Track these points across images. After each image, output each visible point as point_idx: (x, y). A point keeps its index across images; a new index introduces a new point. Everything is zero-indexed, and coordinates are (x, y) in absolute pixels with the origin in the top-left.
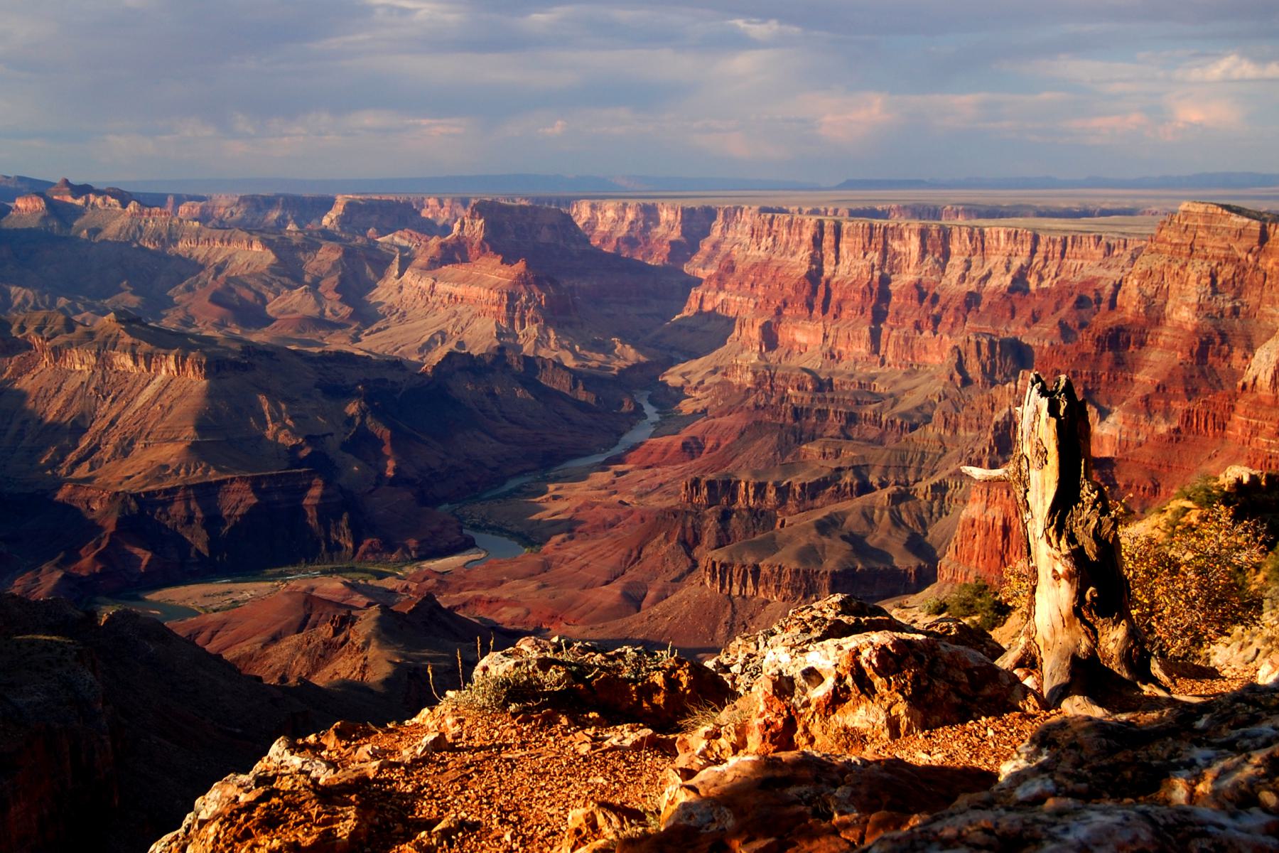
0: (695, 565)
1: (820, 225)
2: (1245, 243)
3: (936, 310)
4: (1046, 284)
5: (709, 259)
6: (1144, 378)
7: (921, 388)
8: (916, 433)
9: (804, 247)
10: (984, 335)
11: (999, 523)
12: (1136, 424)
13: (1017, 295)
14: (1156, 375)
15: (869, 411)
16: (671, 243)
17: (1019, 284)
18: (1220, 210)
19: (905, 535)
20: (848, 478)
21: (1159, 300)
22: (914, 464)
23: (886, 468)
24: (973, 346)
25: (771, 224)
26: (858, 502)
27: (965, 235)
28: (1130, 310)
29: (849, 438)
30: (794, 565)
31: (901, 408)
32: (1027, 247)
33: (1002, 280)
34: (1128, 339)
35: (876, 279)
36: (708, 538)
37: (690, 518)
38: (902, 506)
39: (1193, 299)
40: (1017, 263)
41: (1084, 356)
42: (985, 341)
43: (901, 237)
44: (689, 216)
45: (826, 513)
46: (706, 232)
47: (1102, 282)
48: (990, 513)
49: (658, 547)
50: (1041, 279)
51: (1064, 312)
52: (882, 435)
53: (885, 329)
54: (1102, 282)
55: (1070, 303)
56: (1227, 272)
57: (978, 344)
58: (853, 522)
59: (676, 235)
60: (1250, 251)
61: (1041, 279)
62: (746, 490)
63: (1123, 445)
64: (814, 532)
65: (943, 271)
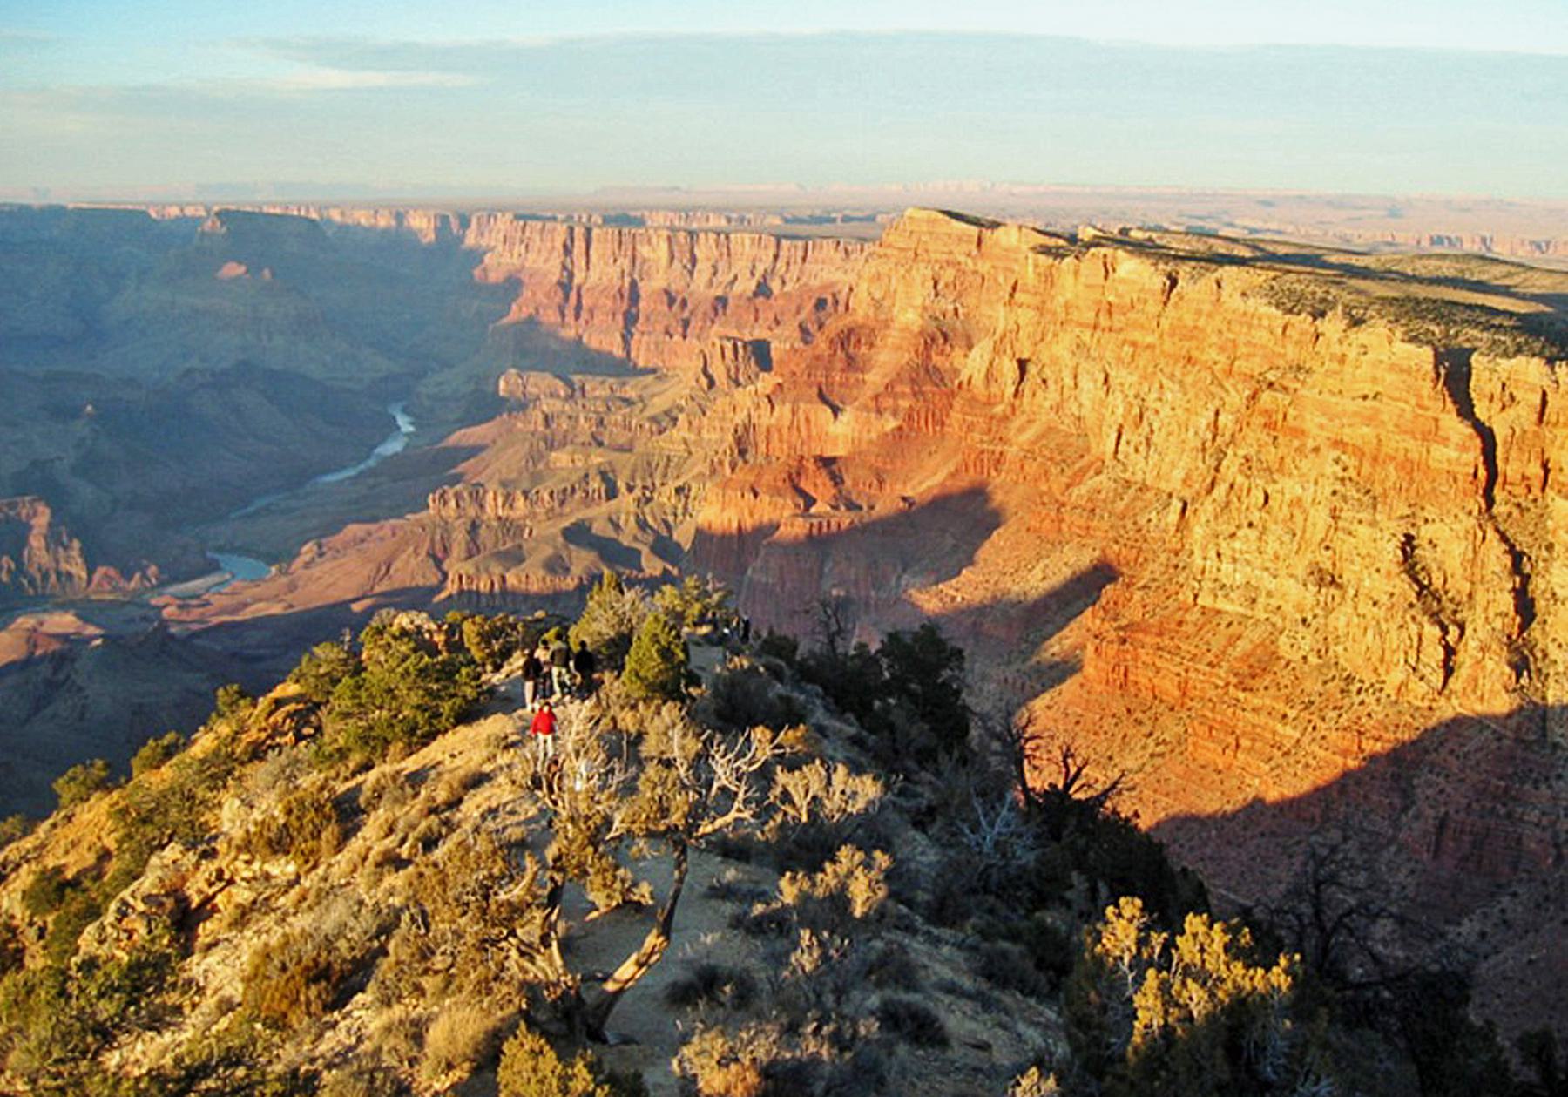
0: (445, 575)
2: (965, 247)
3: (686, 314)
6: (874, 379)
7: (668, 393)
9: (555, 254)
10: (728, 339)
12: (868, 422)
13: (761, 299)
14: (886, 375)
17: (763, 290)
18: (941, 216)
19: (651, 539)
20: (596, 484)
21: (886, 303)
22: (660, 469)
23: (634, 472)
25: (523, 231)
26: (605, 507)
27: (712, 242)
28: (861, 313)
29: (600, 444)
31: (649, 413)
33: (747, 285)
34: (859, 341)
35: (627, 285)
37: (438, 531)
38: (647, 509)
39: (918, 302)
41: (817, 358)
42: (729, 345)
45: (573, 520)
47: (839, 286)
49: (407, 562)
50: (784, 283)
51: (803, 316)
52: (631, 441)
53: (637, 336)
54: (839, 286)
55: (809, 306)
56: (948, 275)
58: (600, 528)
60: (969, 255)
62: (495, 499)
64: (560, 540)
65: (691, 273)
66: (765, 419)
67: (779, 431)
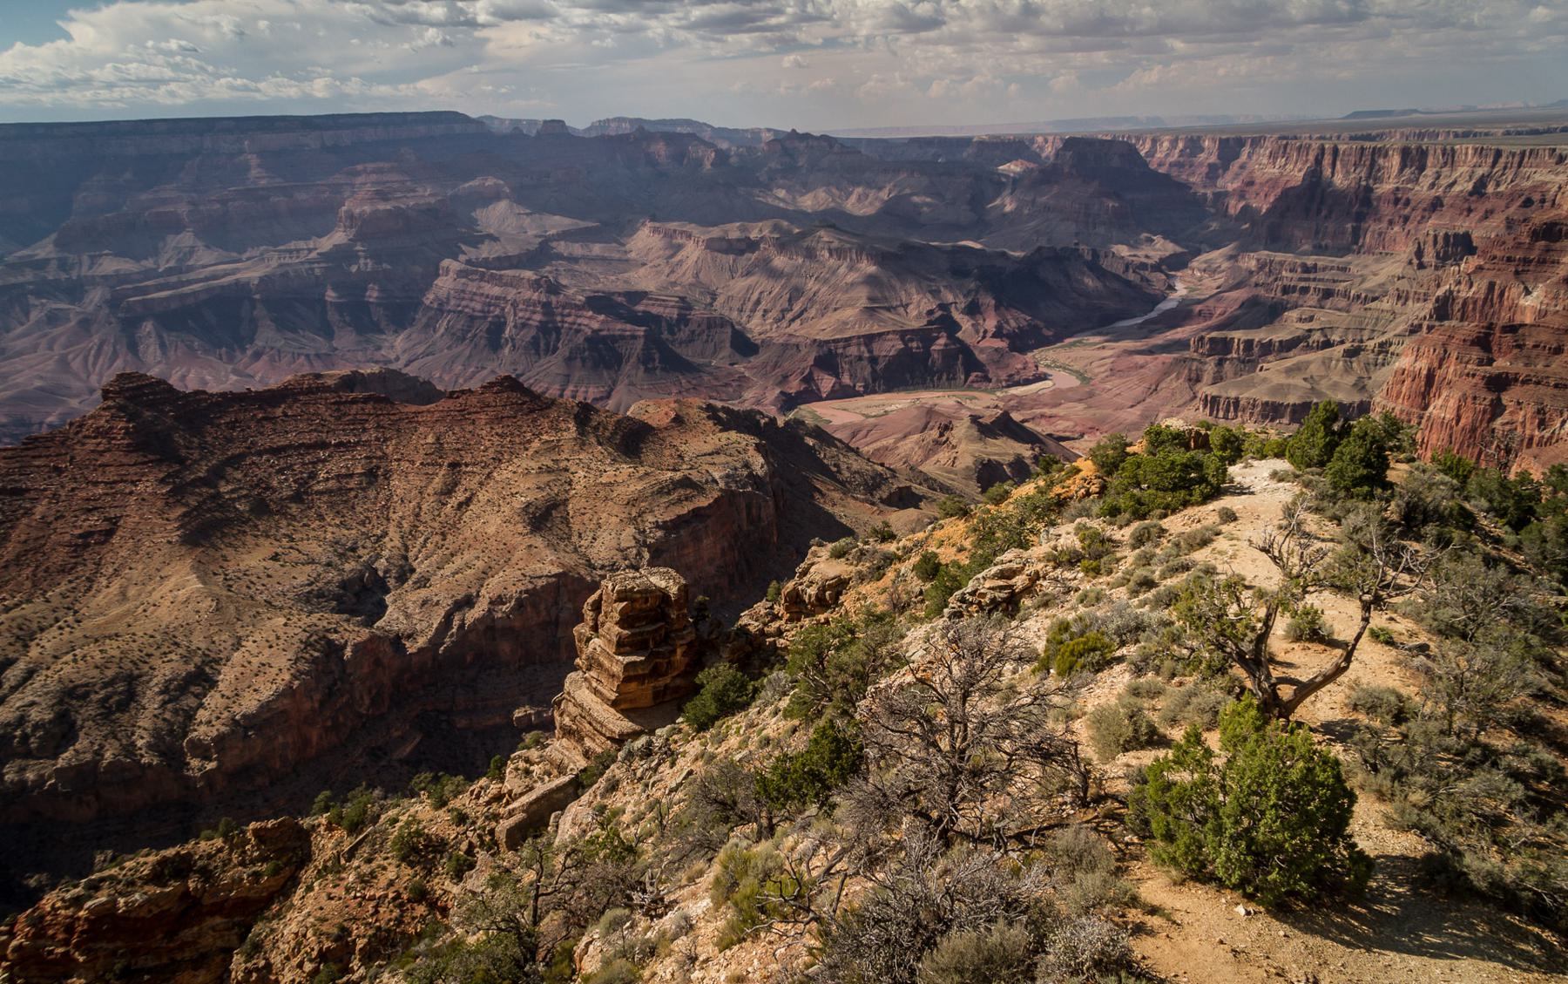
1: (1322, 149)
4: (1501, 188)
5: (1237, 176)
8: (1373, 305)
11: (1424, 372)
15: (1341, 287)
16: (1210, 165)
19: (1351, 379)
24: (1431, 238)
30: (1265, 399)
31: (1367, 285)
32: (1490, 160)
36: (1207, 377)
40: (1480, 172)
41: (1518, 245)
43: (1386, 155)
44: (1224, 144)
46: (1237, 156)
48: (1418, 365)
57: (1436, 237)
59: (1213, 159)
61: (1498, 185)
63: (1542, 314)
66: (1464, 293)
67: (1475, 303)
